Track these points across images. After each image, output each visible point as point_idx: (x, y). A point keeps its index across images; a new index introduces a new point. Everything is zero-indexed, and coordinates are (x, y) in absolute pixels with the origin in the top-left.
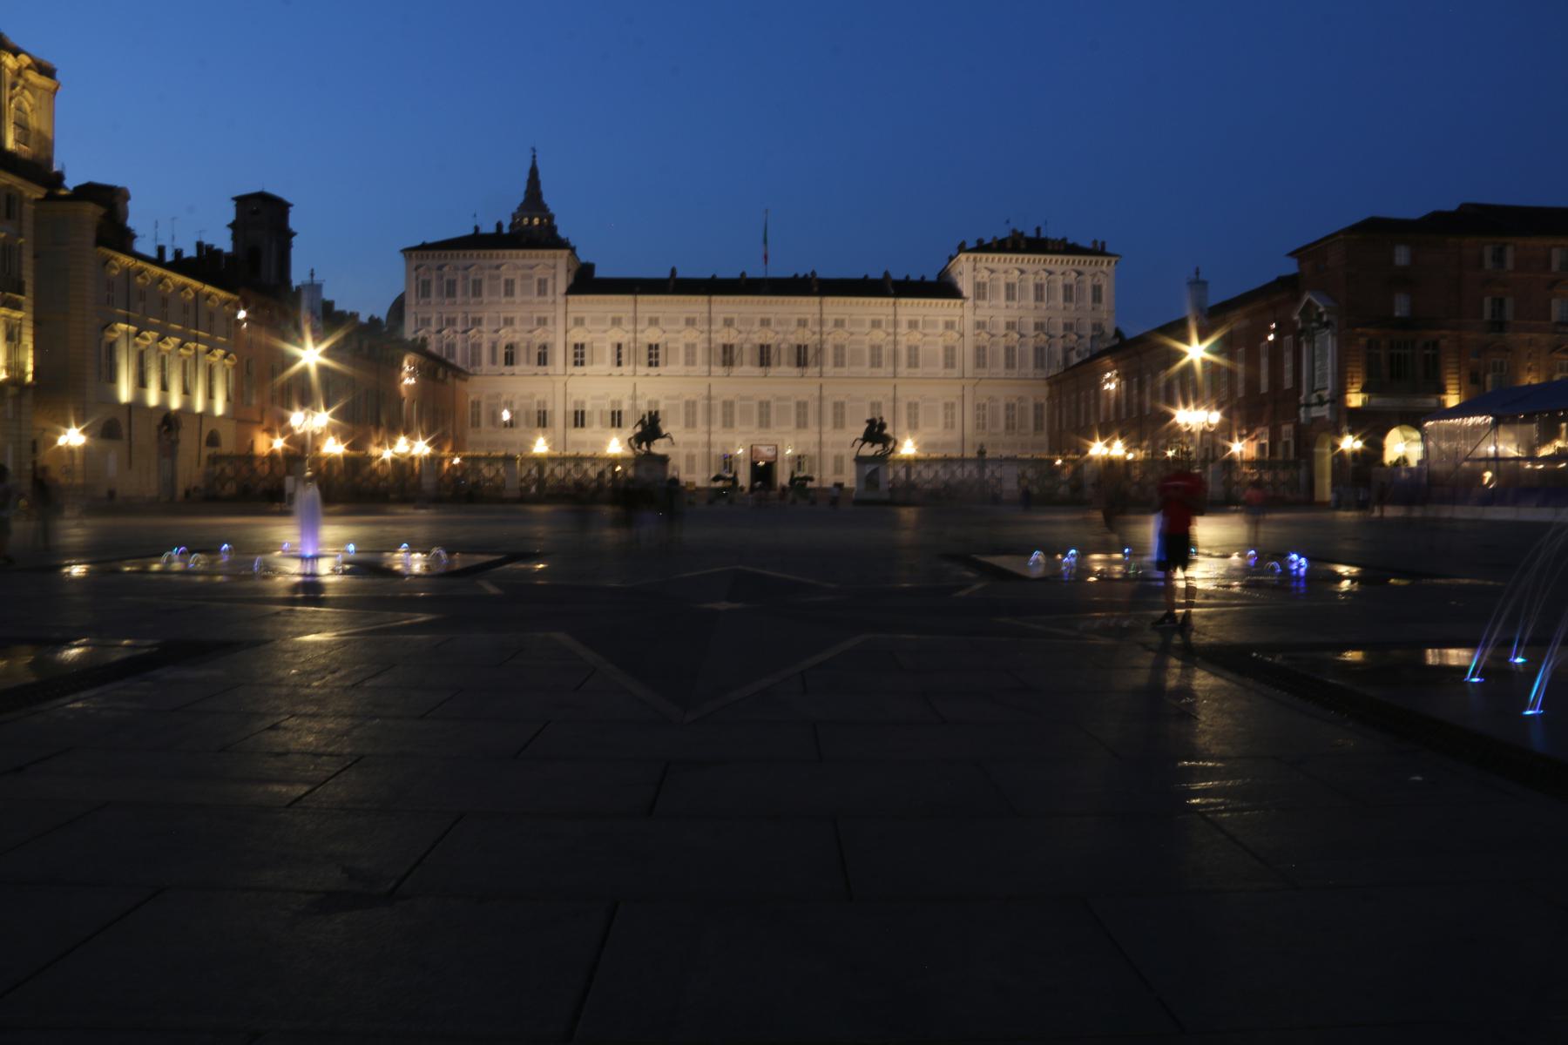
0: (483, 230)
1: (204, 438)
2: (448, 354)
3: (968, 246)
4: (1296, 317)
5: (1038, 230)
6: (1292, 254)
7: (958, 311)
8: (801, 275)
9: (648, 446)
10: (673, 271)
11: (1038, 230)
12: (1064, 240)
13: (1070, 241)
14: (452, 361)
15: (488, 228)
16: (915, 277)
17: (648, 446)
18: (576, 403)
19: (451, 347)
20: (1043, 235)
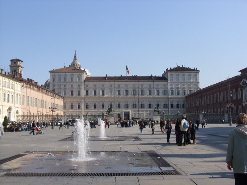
0: (66, 67)
1: (16, 112)
2: (59, 93)
3: (168, 69)
4: (241, 84)
5: (183, 65)
6: (240, 71)
7: (166, 83)
8: (133, 76)
9: (110, 113)
10: (107, 75)
11: (183, 65)
13: (189, 68)
16: (157, 76)
17: (110, 113)
18: (86, 103)
20: (184, 67)
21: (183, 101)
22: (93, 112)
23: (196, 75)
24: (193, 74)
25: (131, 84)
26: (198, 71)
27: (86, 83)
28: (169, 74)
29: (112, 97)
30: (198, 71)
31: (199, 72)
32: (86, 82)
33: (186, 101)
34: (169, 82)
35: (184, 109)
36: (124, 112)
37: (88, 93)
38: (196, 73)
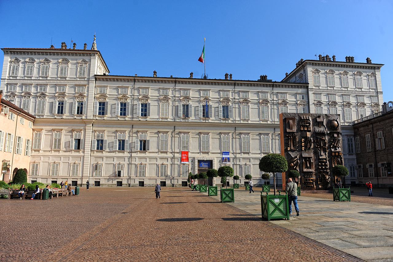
0: (56, 47)
12: (352, 58)
14: (27, 111)
15: (58, 46)
18: (98, 136)
19: (27, 105)
21: (347, 135)
22: (115, 159)
23: (374, 75)
24: (365, 73)
25: (213, 94)
26: (378, 67)
27: (99, 83)
28: (310, 70)
29: (169, 120)
30: (378, 67)
31: (379, 68)
32: (100, 80)
33: (355, 136)
34: (309, 87)
35: (351, 157)
36: (199, 161)
37: (103, 109)
38: (372, 71)
